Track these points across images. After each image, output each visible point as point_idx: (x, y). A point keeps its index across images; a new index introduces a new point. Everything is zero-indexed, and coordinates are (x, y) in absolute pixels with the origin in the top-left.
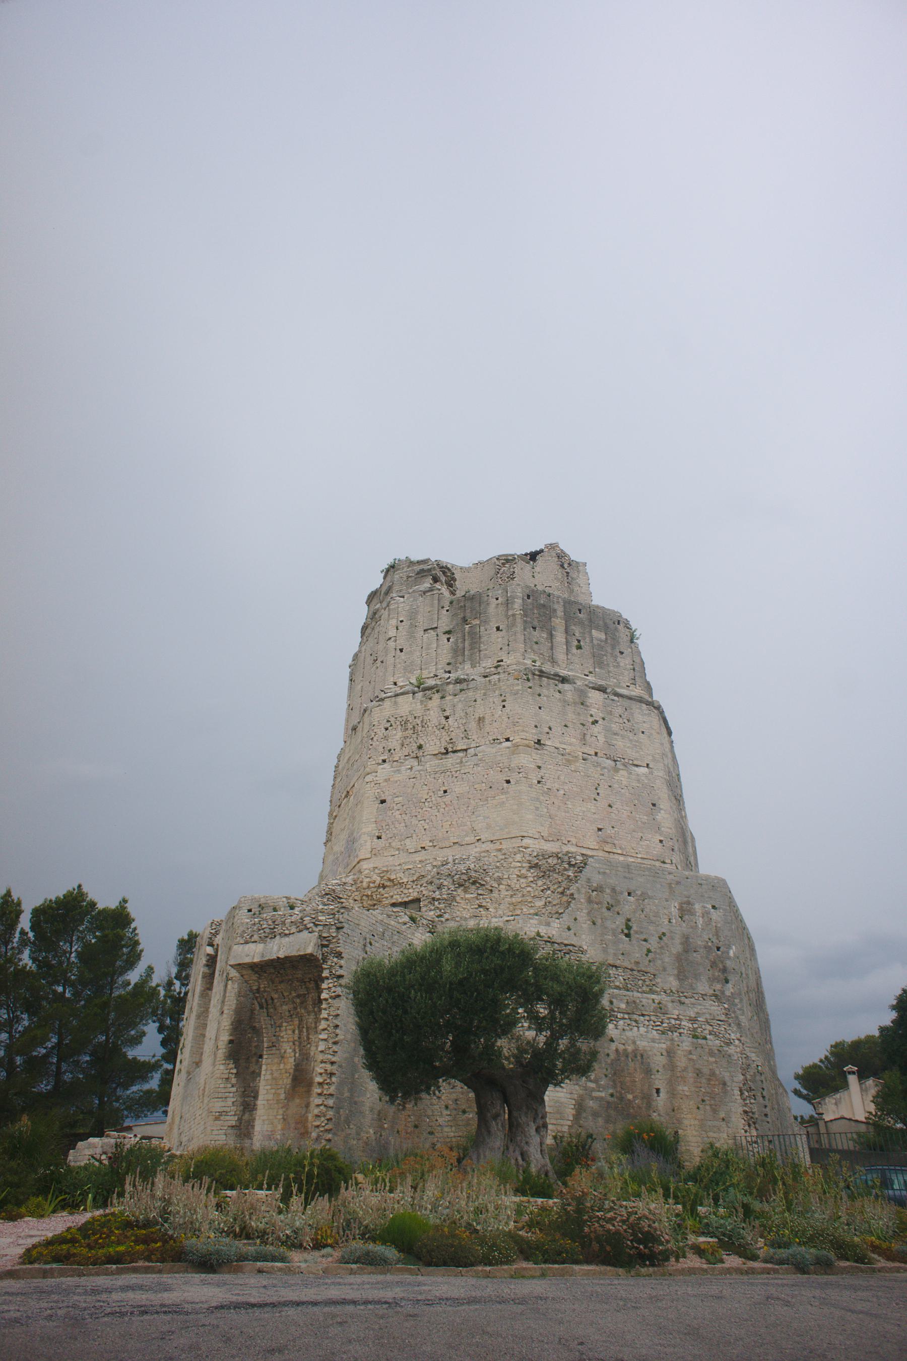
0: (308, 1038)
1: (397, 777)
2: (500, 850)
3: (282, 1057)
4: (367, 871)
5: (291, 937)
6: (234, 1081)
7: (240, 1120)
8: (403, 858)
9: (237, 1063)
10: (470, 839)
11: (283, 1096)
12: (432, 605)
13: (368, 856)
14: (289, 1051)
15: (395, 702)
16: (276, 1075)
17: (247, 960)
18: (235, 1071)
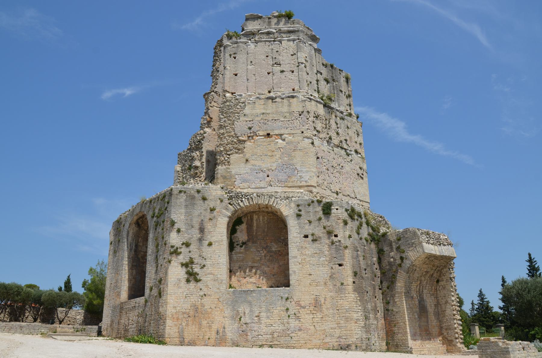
0: (423, 291)
1: (322, 148)
2: (362, 206)
3: (412, 297)
4: (315, 193)
5: (445, 247)
7: (365, 324)
8: (328, 192)
9: (359, 293)
10: (353, 195)
11: (417, 317)
12: (319, 59)
13: (316, 185)
14: (415, 296)
15: (317, 105)
16: (411, 306)
17: (433, 252)
18: (358, 298)
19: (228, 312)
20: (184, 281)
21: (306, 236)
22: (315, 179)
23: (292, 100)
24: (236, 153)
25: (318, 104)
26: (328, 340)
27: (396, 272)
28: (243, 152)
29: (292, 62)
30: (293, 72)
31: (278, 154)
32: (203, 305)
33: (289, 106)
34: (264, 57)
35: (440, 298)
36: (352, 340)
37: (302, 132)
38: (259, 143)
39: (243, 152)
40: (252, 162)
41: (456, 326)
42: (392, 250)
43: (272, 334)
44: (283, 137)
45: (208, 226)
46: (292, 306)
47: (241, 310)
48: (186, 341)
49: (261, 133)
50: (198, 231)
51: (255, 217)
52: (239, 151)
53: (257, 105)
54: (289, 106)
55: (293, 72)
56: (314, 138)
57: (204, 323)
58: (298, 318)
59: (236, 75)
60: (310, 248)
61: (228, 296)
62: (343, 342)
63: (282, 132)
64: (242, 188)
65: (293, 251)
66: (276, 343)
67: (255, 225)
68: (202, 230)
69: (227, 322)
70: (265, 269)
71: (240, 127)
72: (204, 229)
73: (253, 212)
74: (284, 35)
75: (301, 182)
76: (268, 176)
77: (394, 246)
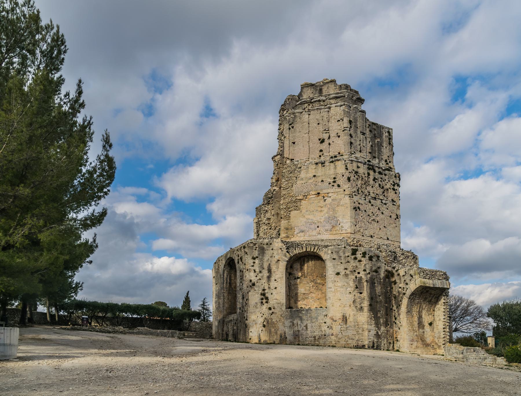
6: (373, 319)
19: (288, 323)
20: (259, 304)
21: (338, 274)
22: (353, 227)
23: (337, 163)
24: (295, 210)
25: (359, 165)
26: (350, 341)
27: (402, 298)
28: (299, 209)
29: (339, 128)
30: (339, 137)
31: (325, 210)
32: (272, 319)
33: (335, 168)
34: (316, 125)
35: (435, 317)
36: (366, 343)
37: (344, 190)
38: (311, 201)
39: (299, 209)
40: (307, 217)
41: (444, 336)
42: (400, 283)
43: (315, 337)
44: (330, 195)
45: (274, 268)
46: (328, 320)
47: (295, 322)
48: (262, 341)
49: (313, 193)
50: (267, 271)
51: (306, 260)
52: (297, 208)
53: (310, 169)
54: (335, 168)
55: (339, 137)
56: (354, 194)
57: (273, 330)
58: (331, 328)
59: (294, 143)
60: (340, 281)
61: (287, 313)
62: (360, 343)
63: (329, 191)
64: (297, 238)
65: (329, 284)
66: (317, 343)
67: (306, 265)
68: (270, 271)
69: (287, 330)
70: (313, 295)
71: (298, 188)
72: (271, 270)
73: (305, 256)
74: (332, 101)
75: (342, 231)
76: (318, 227)
77: (403, 280)
